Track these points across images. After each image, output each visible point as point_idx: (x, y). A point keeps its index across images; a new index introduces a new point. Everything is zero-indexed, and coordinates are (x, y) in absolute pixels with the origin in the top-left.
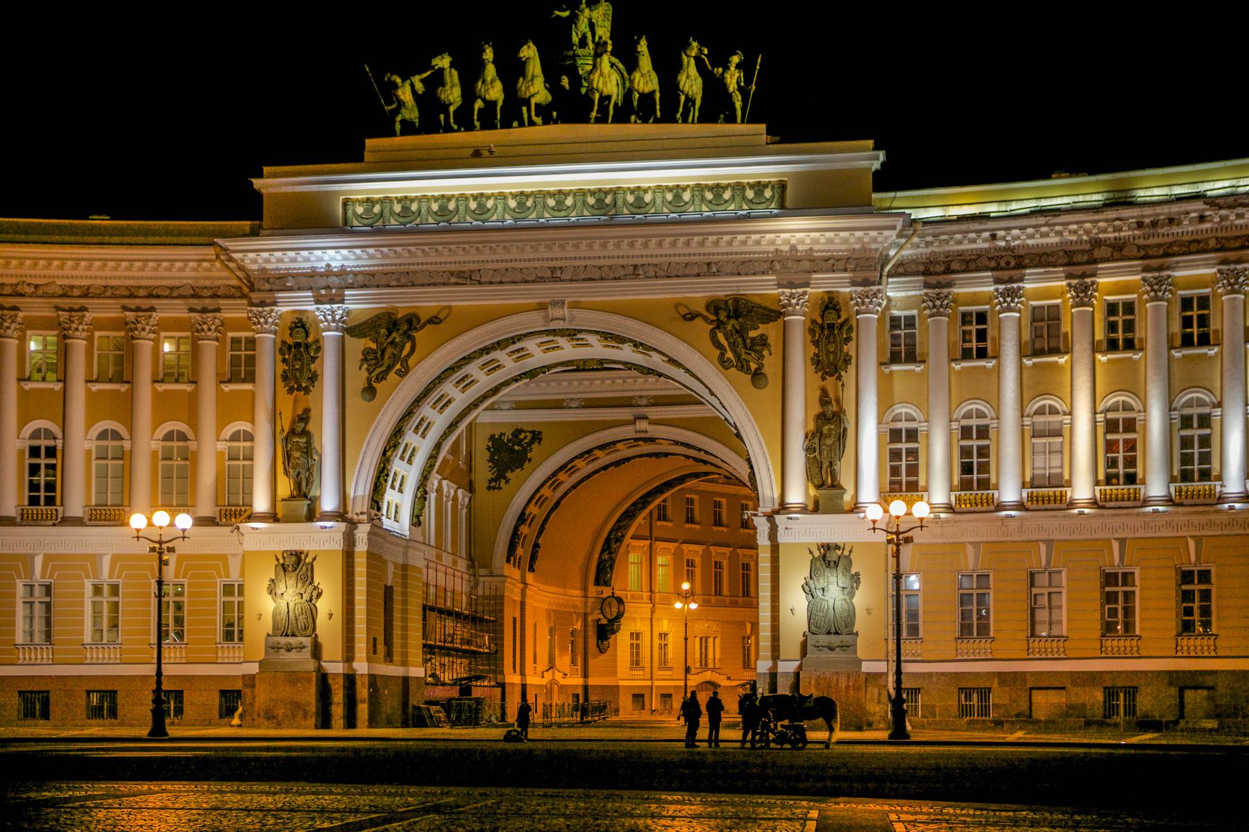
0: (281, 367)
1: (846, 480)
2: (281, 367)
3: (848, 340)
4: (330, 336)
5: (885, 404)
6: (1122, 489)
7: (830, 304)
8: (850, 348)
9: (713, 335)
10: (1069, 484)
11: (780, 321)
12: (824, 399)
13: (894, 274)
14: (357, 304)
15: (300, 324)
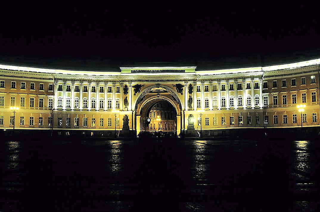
0: (124, 91)
1: (192, 106)
2: (124, 91)
3: (192, 89)
4: (130, 88)
5: (197, 97)
6: (224, 107)
7: (190, 85)
8: (193, 90)
9: (177, 89)
10: (218, 107)
11: (185, 87)
12: (190, 97)
13: (198, 81)
14: (134, 84)
15: (126, 86)
